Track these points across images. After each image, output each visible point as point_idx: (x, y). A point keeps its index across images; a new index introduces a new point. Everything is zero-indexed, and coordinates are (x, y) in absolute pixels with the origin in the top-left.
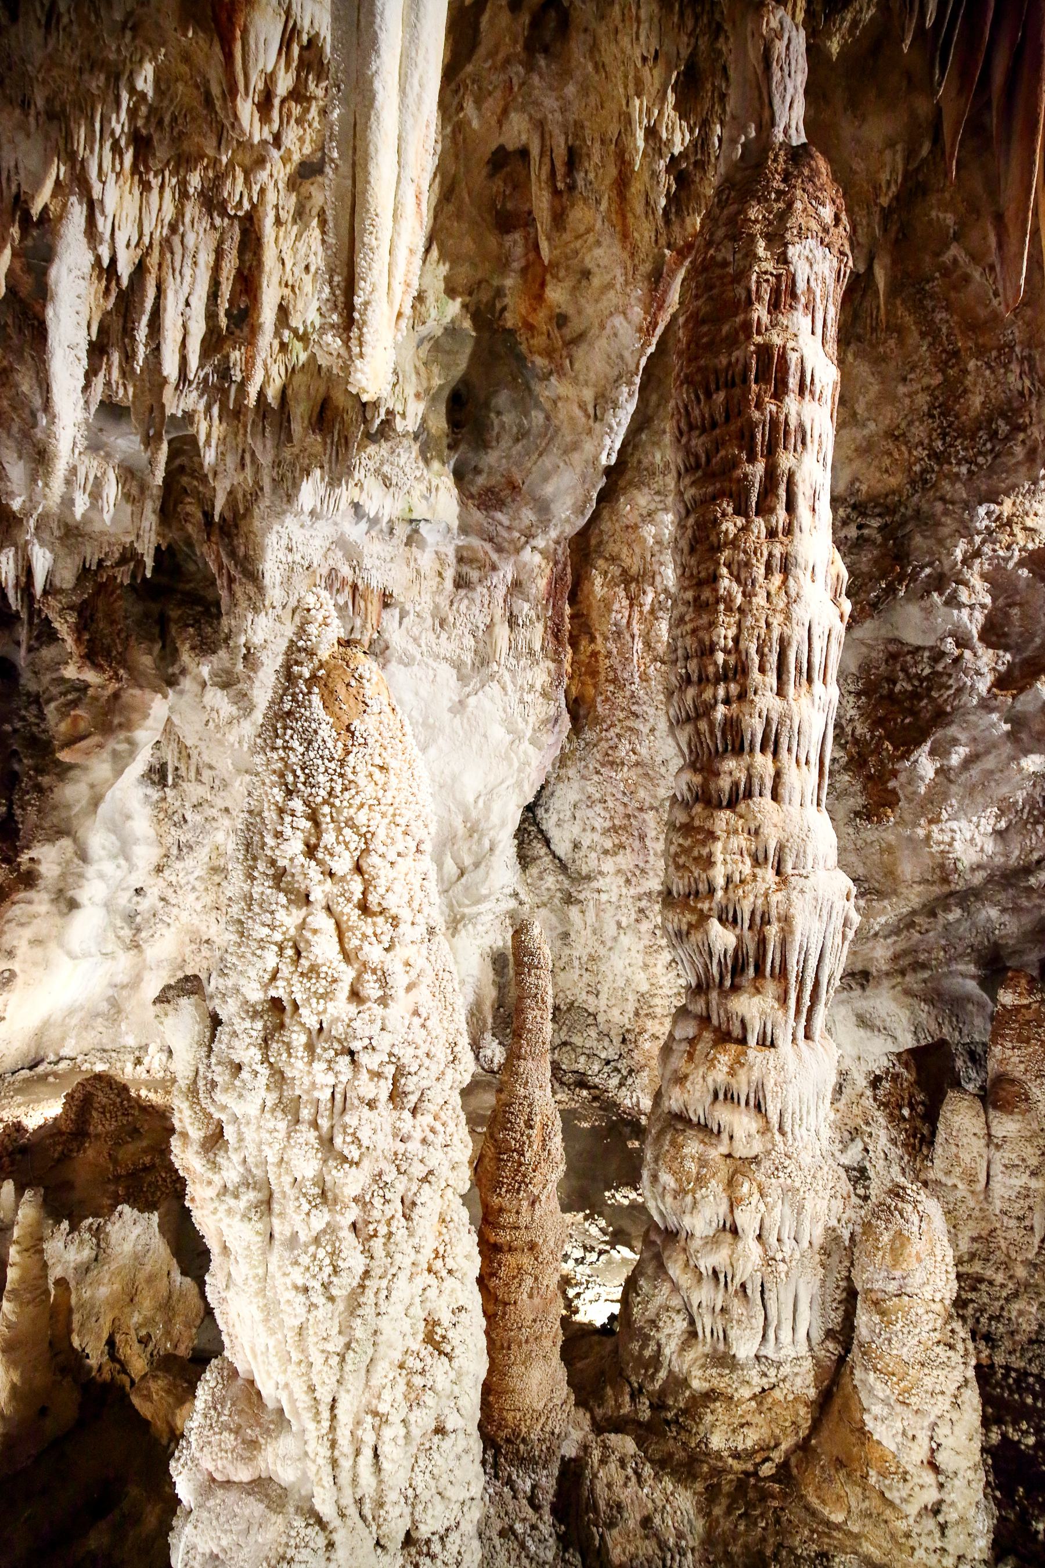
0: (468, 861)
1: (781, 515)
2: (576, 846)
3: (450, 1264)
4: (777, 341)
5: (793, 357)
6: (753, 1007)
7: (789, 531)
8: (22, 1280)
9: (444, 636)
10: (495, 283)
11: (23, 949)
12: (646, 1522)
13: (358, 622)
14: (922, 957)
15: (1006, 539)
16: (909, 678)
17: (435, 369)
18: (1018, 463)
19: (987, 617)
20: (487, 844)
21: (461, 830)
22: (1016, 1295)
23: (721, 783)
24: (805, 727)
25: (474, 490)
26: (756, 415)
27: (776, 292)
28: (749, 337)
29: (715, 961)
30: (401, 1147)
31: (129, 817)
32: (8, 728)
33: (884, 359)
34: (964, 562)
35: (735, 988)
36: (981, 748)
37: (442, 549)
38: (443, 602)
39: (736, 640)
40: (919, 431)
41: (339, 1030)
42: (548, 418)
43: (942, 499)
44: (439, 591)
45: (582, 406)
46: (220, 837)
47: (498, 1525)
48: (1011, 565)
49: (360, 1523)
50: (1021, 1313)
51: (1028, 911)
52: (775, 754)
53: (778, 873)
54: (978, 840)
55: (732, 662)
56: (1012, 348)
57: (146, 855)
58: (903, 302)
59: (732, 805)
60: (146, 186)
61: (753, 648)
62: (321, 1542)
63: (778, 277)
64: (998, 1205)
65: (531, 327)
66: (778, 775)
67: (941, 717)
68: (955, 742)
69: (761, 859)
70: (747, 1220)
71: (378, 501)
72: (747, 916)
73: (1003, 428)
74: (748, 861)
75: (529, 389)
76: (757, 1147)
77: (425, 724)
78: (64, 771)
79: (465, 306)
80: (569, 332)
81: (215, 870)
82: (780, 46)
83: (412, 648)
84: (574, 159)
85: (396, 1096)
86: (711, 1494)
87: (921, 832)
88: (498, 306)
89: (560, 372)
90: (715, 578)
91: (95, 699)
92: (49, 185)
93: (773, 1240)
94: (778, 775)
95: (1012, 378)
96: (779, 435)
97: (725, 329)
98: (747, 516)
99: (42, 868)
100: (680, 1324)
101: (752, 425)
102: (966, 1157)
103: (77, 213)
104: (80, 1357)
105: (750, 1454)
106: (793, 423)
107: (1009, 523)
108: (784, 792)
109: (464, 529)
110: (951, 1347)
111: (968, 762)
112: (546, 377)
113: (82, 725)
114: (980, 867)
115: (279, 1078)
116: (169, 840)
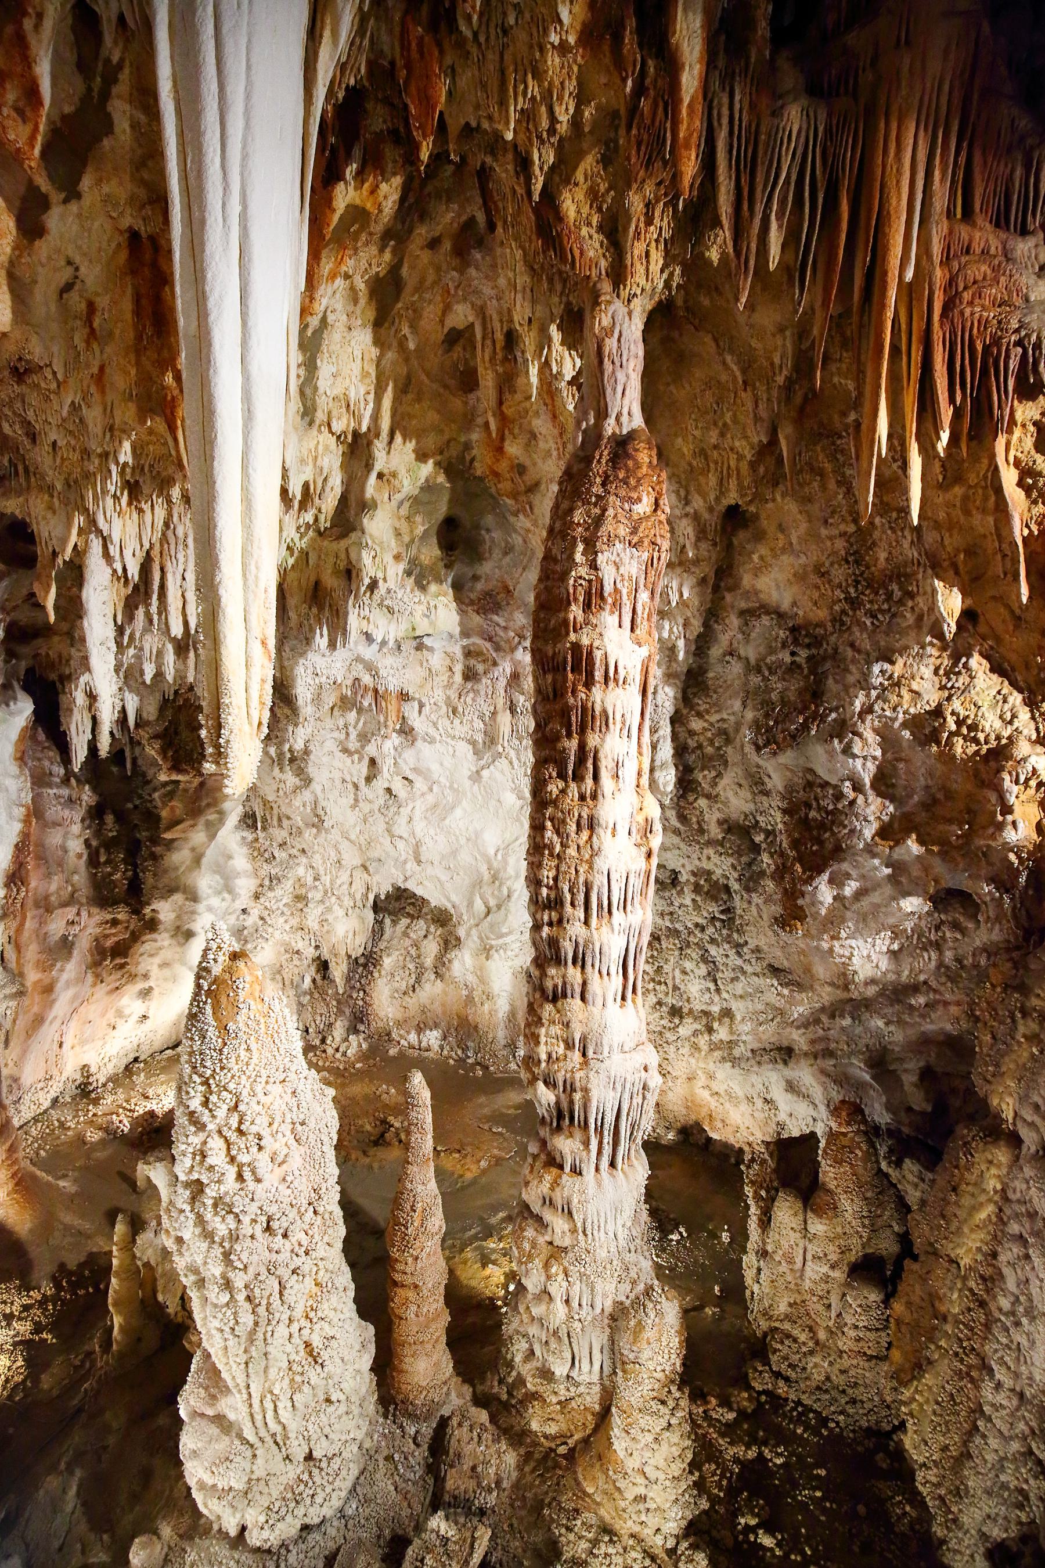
0: (492, 903)
1: (589, 782)
3: (320, 1314)
4: (585, 641)
5: (598, 655)
6: (566, 1146)
7: (594, 797)
8: (120, 1266)
9: (457, 721)
10: (463, 439)
11: (155, 971)
12: (474, 1468)
13: (382, 719)
14: (833, 1045)
15: (894, 699)
16: (819, 809)
17: (418, 519)
19: (879, 768)
20: (505, 892)
21: (486, 877)
22: (811, 1353)
24: (605, 949)
25: (473, 596)
26: (571, 701)
27: (588, 594)
28: (568, 634)
30: (274, 1256)
31: (230, 857)
32: (130, 806)
33: (810, 500)
34: (860, 714)
35: (559, 1129)
36: (869, 884)
37: (449, 650)
38: (454, 696)
39: (556, 879)
40: (839, 574)
41: (227, 1200)
43: (852, 645)
44: (449, 685)
46: (301, 871)
47: (385, 1453)
48: (897, 725)
49: (275, 1447)
50: (816, 1365)
51: (913, 1025)
52: (583, 967)
53: (584, 1055)
54: (874, 957)
57: (245, 886)
58: (823, 449)
59: (554, 1000)
60: (141, 511)
62: (249, 1453)
63: (590, 581)
64: (807, 1284)
65: (496, 474)
66: (584, 984)
67: (838, 852)
68: (848, 876)
71: (384, 628)
74: (562, 1045)
76: (567, 1242)
77: (451, 787)
78: (169, 845)
79: (437, 464)
80: (529, 478)
81: (299, 898)
82: (611, 344)
83: (432, 731)
85: (268, 1228)
86: (528, 1457)
87: (825, 946)
88: (468, 458)
91: (186, 790)
92: (75, 531)
93: (575, 1304)
94: (584, 984)
99: (162, 917)
100: (524, 1345)
102: (785, 1245)
103: (96, 546)
104: (162, 1307)
105: (554, 1438)
106: (598, 709)
107: (898, 684)
108: (589, 997)
109: (465, 634)
110: (663, 1403)
111: (859, 894)
113: (178, 812)
114: (873, 981)
115: (200, 1221)
116: (263, 873)
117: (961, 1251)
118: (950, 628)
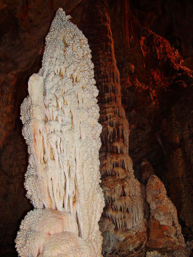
2: (11, 166)
23: (106, 98)
29: (109, 135)
35: (114, 142)
39: (105, 71)
66: (116, 97)
69: (116, 113)
70: (126, 190)
72: (115, 124)
73: (121, 66)
90: (99, 60)
117: (179, 174)
118: (133, 71)
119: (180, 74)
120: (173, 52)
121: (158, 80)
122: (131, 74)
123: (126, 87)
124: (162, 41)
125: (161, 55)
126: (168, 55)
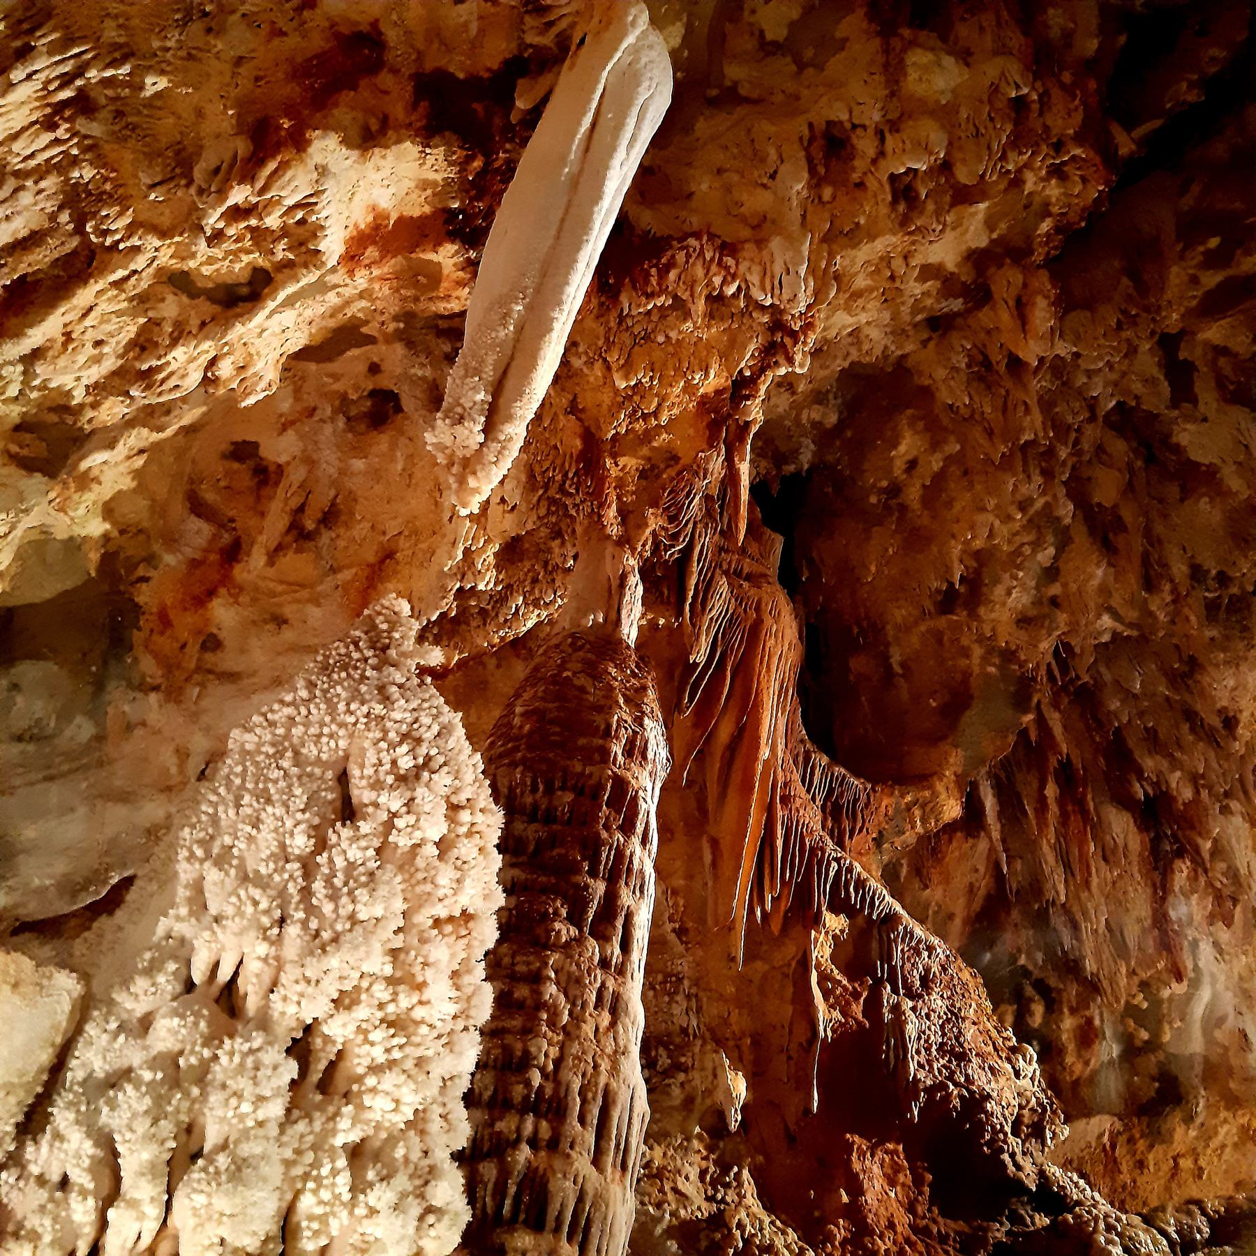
10: (156, 547)
18: (672, 1108)
26: (604, 835)
39: (558, 1062)
42: (100, 738)
45: (183, 755)
55: (549, 1091)
56: (680, 980)
61: (576, 1085)
65: (165, 621)
75: (99, 686)
79: (106, 537)
84: (330, 517)
89: (173, 694)
90: (536, 979)
95: (676, 1010)
96: (619, 870)
97: (582, 741)
98: (581, 931)
101: (597, 843)
112: (146, 688)
118: (735, 1119)
119: (1042, 1221)
120: (1009, 1060)
121: (891, 1226)
122: (716, 1128)
123: (667, 1216)
124: (944, 969)
125: (928, 1049)
126: (974, 1068)
